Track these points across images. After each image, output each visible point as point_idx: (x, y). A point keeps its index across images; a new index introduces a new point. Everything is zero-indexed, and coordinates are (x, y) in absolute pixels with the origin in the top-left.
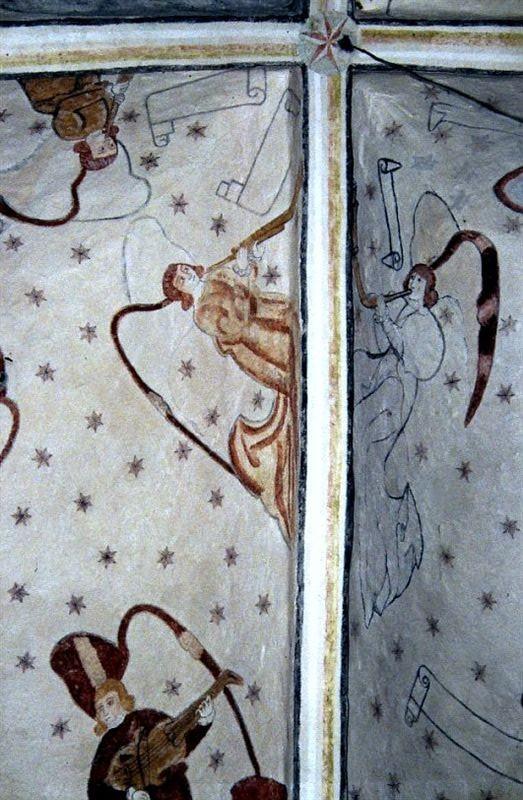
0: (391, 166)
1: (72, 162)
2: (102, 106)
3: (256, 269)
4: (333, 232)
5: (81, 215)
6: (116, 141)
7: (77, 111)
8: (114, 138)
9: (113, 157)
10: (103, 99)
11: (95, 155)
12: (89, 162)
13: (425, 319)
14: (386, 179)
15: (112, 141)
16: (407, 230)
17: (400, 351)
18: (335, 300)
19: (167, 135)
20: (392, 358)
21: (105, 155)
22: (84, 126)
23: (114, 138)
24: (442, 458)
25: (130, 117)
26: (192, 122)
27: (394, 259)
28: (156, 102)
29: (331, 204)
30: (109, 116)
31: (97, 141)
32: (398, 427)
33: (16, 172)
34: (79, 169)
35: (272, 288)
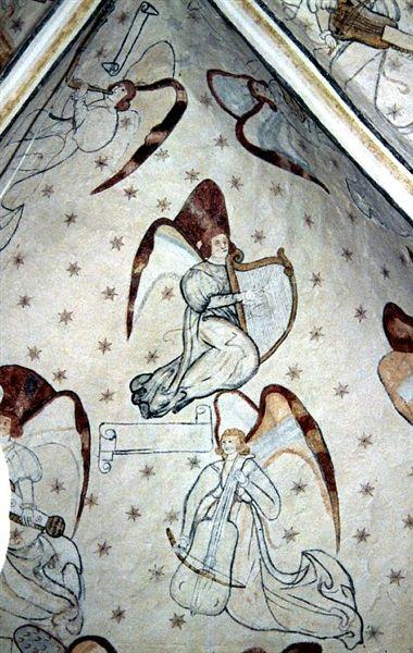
0: (150, 10)
3: (13, 12)
4: (63, 35)
13: (111, 116)
14: (142, 17)
16: (135, 56)
17: (78, 124)
18: (33, 77)
20: (69, 125)
24: (64, 199)
27: (114, 67)
29: (75, 15)
32: (41, 168)
35: (11, 32)
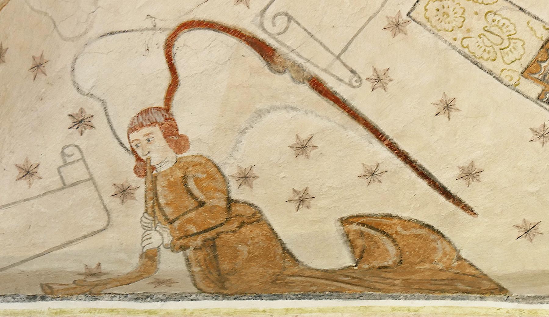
1: (185, 122)
2: (168, 210)
5: (162, 38)
6: (134, 152)
7: (202, 204)
8: (139, 159)
9: (132, 129)
10: (171, 222)
11: (157, 132)
12: (162, 118)
15: (139, 152)
19: (66, 164)
21: (145, 130)
22: (184, 177)
23: (139, 159)
25: (124, 192)
26: (37, 186)
28: (93, 218)
30: (153, 194)
31: (161, 154)
33: (259, 106)
34: (175, 109)
